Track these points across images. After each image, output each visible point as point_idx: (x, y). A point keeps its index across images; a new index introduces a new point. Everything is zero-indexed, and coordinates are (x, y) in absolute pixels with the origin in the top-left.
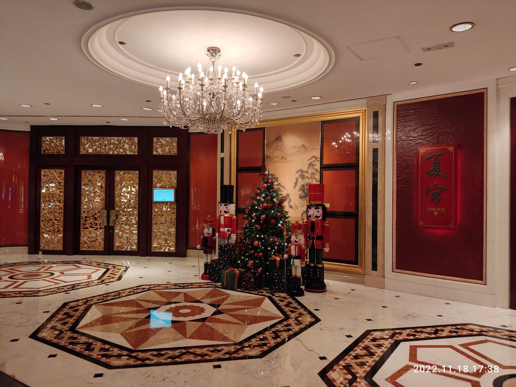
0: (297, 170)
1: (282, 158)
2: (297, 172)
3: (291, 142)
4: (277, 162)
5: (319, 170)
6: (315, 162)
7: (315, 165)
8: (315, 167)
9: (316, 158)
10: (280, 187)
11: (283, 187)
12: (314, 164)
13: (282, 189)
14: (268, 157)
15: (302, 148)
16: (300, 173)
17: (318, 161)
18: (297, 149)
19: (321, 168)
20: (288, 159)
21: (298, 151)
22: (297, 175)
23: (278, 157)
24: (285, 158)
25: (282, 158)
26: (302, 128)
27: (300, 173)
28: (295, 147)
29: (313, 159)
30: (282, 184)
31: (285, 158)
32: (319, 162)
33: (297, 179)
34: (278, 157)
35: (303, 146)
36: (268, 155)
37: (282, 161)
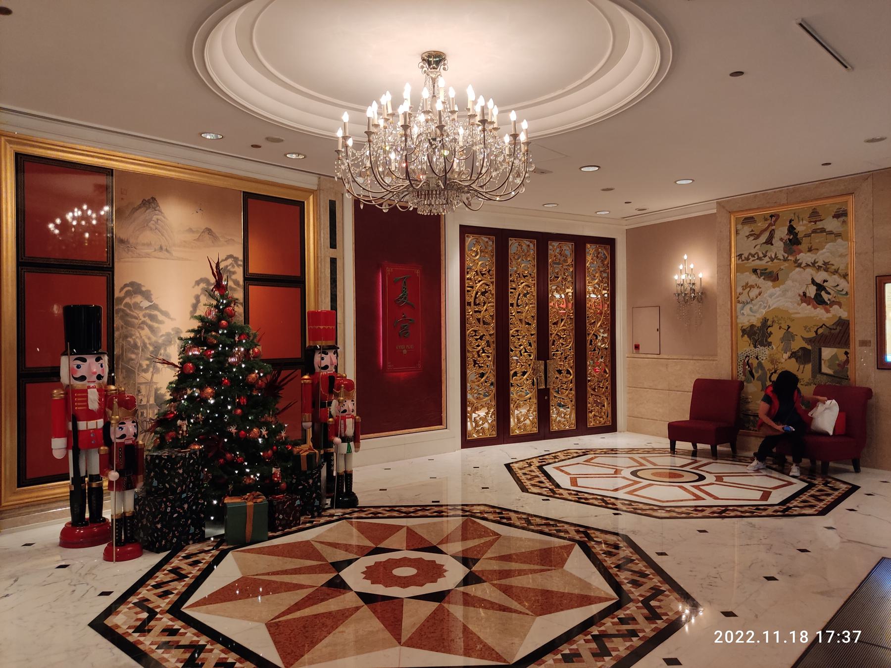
0: (198, 279)
1: (161, 248)
2: (197, 283)
3: (175, 216)
4: (148, 255)
5: (241, 283)
6: (233, 267)
7: (234, 273)
8: (234, 277)
9: (236, 259)
10: (156, 312)
11: (166, 314)
12: (232, 270)
13: (161, 317)
14: (122, 241)
15: (207, 236)
16: (203, 285)
17: (238, 266)
18: (197, 236)
19: (245, 279)
20: (174, 253)
21: (198, 240)
22: (198, 290)
23: (149, 245)
24: (167, 250)
25: (161, 248)
26: (204, 195)
27: (203, 285)
28: (190, 230)
29: (230, 261)
30: (163, 307)
31: (167, 250)
32: (241, 269)
33: (197, 298)
34: (149, 245)
35: (209, 231)
36: (123, 236)
37: (160, 254)
